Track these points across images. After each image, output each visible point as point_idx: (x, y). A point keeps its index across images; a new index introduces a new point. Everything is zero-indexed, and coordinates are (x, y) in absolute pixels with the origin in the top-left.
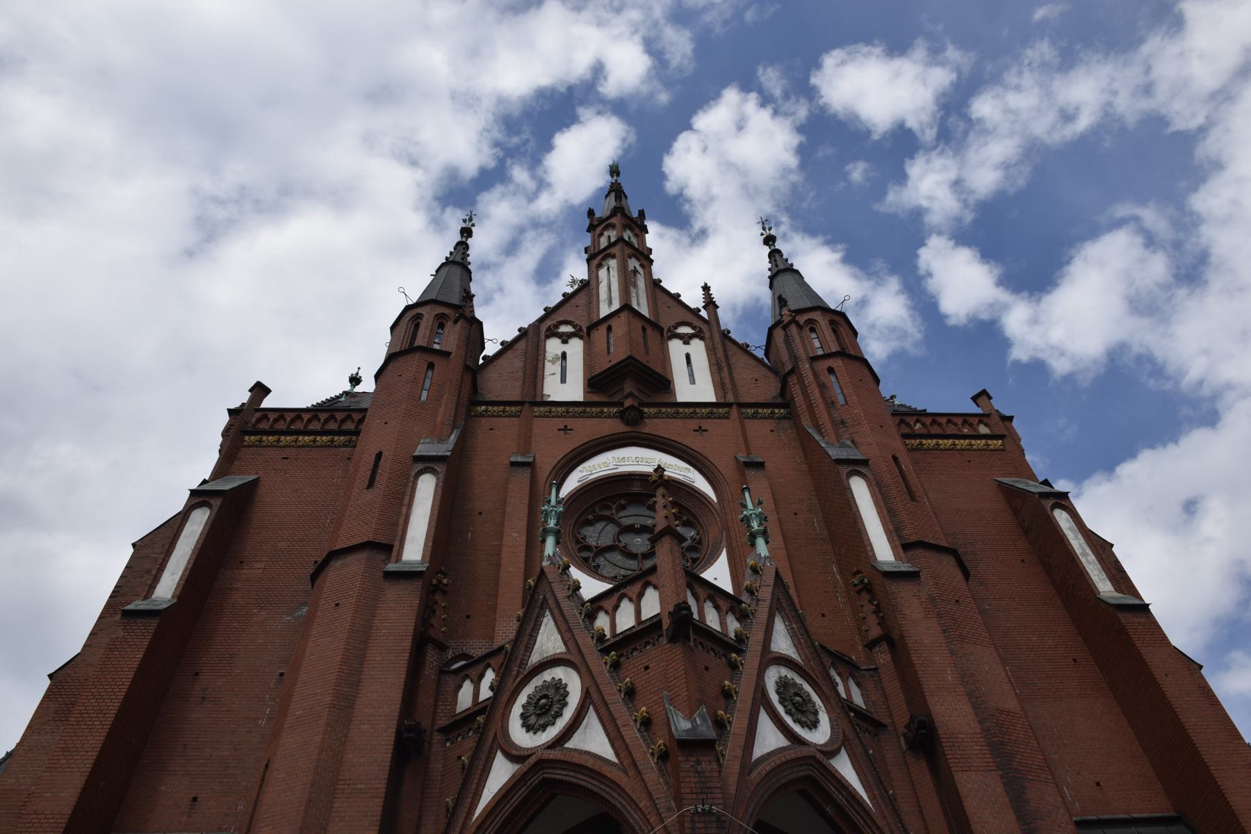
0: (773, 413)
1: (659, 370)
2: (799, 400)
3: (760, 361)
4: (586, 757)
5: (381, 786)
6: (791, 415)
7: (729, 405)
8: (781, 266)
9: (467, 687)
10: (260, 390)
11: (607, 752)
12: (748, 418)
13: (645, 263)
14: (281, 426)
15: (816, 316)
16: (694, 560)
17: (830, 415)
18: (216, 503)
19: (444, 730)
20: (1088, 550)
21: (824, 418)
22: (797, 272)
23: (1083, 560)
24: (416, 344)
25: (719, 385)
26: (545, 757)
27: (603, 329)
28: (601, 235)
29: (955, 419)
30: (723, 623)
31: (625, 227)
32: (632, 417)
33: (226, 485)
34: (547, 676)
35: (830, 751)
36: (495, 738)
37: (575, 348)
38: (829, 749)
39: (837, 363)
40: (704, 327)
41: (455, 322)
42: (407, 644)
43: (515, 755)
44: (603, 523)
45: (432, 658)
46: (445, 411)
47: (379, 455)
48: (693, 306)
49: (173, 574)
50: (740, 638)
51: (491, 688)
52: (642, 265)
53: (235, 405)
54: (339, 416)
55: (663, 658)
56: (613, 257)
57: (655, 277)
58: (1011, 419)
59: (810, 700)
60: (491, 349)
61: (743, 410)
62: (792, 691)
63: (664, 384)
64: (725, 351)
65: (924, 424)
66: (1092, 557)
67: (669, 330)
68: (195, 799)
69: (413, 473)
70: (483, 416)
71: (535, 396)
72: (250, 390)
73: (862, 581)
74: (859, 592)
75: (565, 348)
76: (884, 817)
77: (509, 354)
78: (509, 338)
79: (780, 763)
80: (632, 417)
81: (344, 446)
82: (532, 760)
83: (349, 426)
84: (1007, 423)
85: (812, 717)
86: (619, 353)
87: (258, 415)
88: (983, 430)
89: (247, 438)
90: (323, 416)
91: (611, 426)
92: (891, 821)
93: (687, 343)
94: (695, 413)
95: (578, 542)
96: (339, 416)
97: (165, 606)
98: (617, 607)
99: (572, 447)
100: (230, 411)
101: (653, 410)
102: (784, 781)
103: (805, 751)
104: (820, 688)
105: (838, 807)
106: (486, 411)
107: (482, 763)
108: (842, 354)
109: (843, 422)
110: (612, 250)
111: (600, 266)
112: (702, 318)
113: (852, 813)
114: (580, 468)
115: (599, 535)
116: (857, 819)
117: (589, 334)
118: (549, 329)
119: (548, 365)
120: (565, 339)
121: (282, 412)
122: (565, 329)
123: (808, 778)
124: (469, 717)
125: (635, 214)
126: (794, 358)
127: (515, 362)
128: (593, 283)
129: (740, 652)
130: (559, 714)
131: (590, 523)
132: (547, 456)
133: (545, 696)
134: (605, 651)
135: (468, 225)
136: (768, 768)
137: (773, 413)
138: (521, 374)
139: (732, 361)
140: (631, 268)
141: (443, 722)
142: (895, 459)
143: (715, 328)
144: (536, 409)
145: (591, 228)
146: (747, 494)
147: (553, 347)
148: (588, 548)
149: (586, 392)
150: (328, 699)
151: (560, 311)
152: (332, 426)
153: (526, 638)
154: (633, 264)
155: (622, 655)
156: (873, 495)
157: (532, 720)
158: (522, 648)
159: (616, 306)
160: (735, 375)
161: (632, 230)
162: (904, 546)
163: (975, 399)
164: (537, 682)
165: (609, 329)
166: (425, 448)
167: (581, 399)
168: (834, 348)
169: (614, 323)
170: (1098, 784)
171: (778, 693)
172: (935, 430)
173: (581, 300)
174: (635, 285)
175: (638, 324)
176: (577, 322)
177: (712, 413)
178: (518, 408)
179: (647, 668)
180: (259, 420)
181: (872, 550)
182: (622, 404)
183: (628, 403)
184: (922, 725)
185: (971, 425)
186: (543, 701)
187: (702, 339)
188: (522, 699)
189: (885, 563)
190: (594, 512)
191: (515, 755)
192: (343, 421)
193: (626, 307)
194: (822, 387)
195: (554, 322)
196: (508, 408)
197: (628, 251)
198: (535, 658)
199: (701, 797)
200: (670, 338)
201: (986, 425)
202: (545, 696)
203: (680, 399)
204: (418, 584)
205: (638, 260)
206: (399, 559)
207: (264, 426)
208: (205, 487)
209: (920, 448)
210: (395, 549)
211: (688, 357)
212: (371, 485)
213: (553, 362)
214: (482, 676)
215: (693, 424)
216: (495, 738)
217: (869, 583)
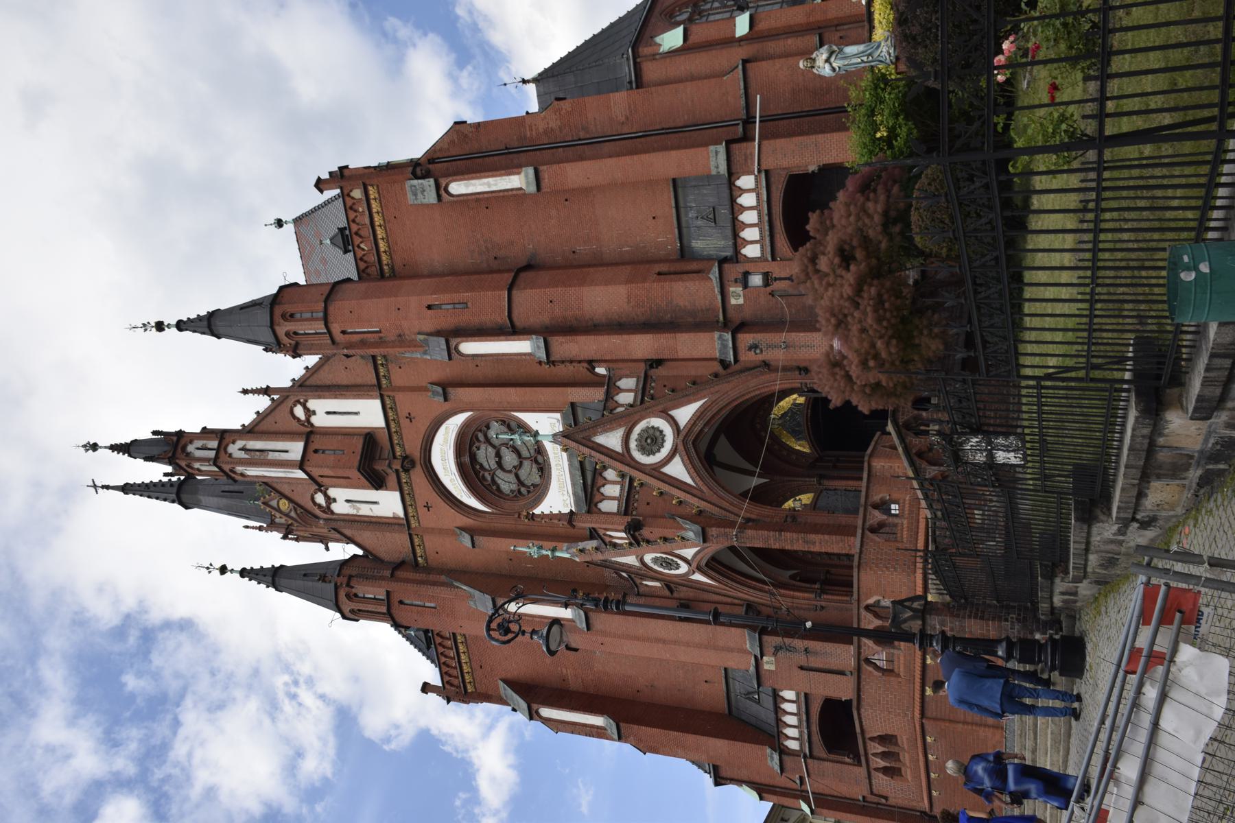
1: (358, 444)
10: (426, 688)
18: (535, 706)
23: (494, 188)
32: (408, 463)
33: (524, 705)
63: (369, 437)
66: (491, 180)
70: (426, 559)
79: (690, 465)
80: (408, 463)
91: (418, 475)
103: (681, 447)
115: (506, 483)
116: (709, 415)
118: (324, 512)
119: (361, 513)
131: (498, 487)
140: (242, 455)
141: (667, 593)
142: (429, 307)
180: (452, 685)
182: (397, 471)
193: (301, 465)
200: (312, 425)
211: (328, 413)
213: (358, 509)
215: (404, 423)
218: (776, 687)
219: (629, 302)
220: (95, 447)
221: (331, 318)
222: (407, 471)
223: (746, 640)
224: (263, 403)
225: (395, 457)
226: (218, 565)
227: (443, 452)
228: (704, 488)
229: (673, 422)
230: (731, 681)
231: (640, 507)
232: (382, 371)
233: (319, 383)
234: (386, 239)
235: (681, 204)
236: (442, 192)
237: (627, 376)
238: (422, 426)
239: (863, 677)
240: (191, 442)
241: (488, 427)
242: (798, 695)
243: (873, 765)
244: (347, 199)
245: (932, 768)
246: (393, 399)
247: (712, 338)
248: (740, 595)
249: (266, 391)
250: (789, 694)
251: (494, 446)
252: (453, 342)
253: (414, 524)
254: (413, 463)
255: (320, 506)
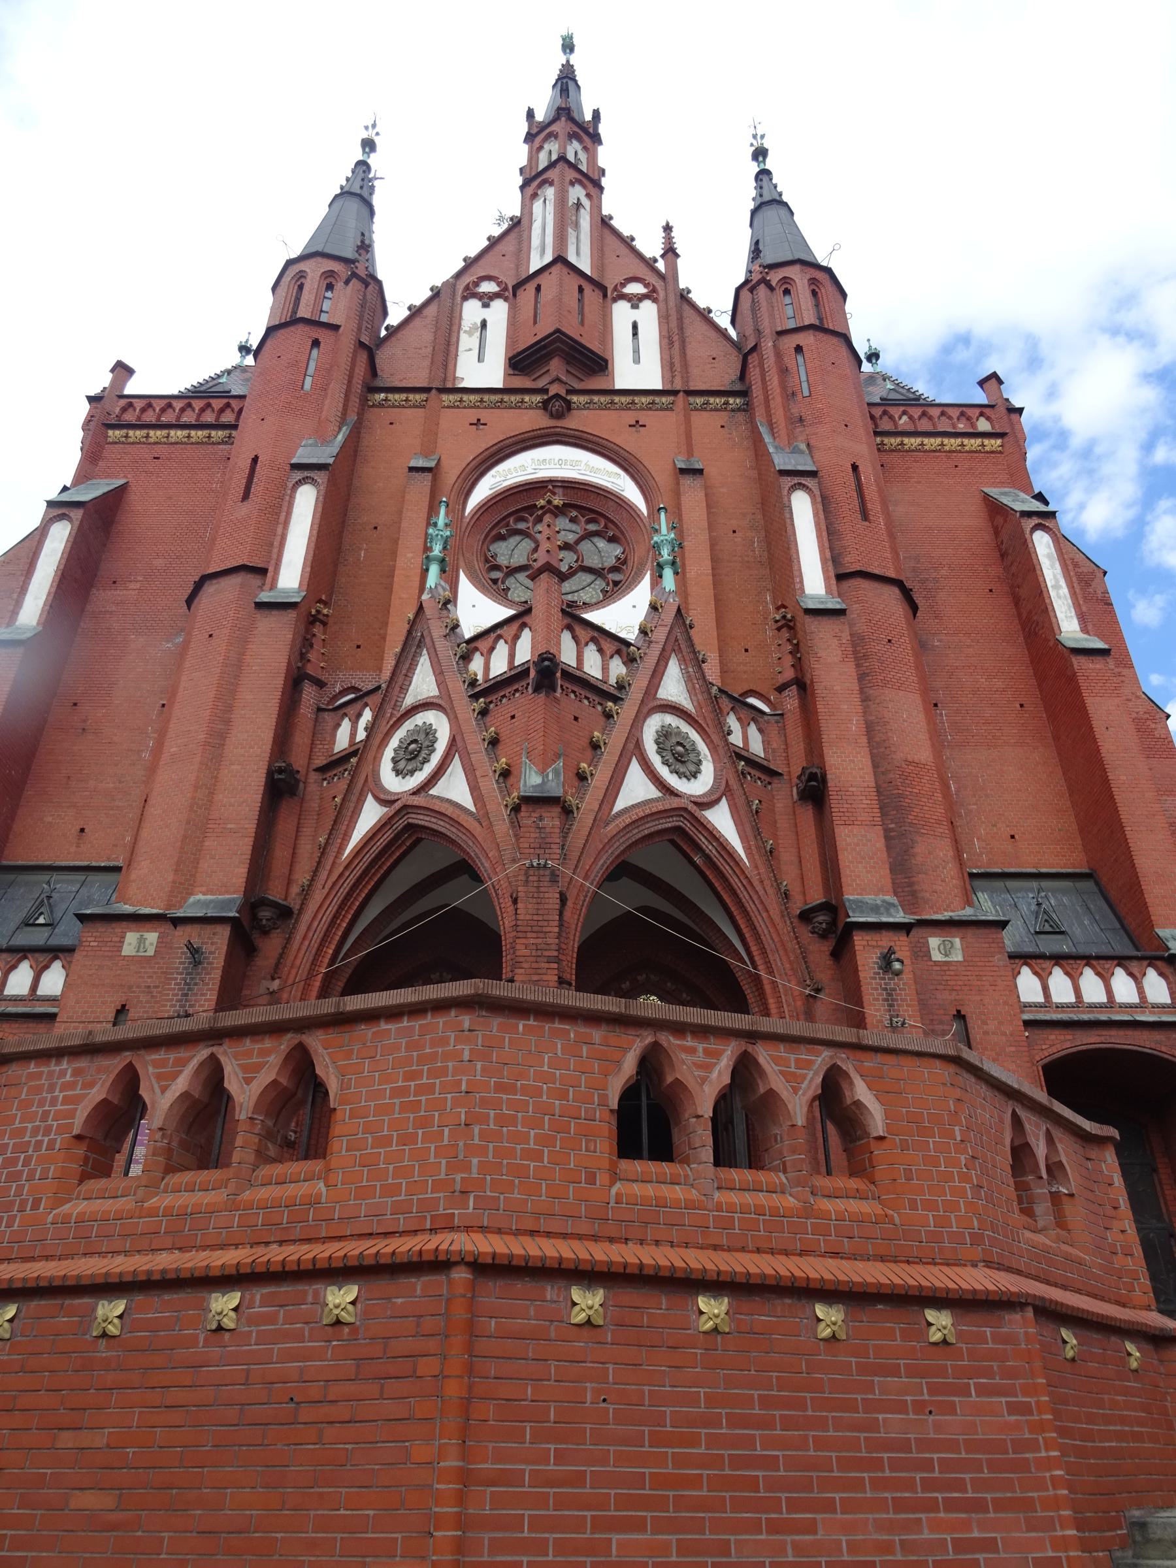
0: (727, 403)
1: (594, 346)
2: (757, 391)
3: (723, 333)
4: (446, 805)
5: (251, 826)
6: (747, 408)
7: (675, 393)
8: (767, 198)
9: (346, 725)
10: (122, 370)
11: (467, 802)
12: (696, 410)
13: (593, 191)
14: (150, 417)
15: (793, 272)
16: (616, 583)
17: (786, 409)
18: (77, 514)
19: (322, 770)
20: (1062, 583)
21: (779, 415)
22: (786, 204)
23: (1053, 594)
24: (298, 316)
25: (668, 367)
26: (410, 803)
27: (531, 287)
28: (541, 148)
29: (950, 411)
30: (605, 669)
31: (572, 136)
33: (86, 494)
34: (420, 719)
35: (707, 803)
36: (366, 780)
37: (499, 312)
38: (705, 800)
39: (807, 340)
40: (659, 284)
41: (347, 282)
42: (279, 682)
43: (385, 800)
44: (518, 538)
45: (309, 693)
46: (332, 404)
47: (255, 460)
48: (648, 254)
49: (36, 598)
50: (621, 686)
51: (366, 729)
52: (588, 195)
53: (95, 391)
54: (217, 404)
55: (525, 705)
56: (551, 184)
57: (605, 212)
58: (1020, 411)
59: (695, 750)
60: (396, 316)
61: (691, 399)
62: (674, 740)
63: (599, 364)
64: (680, 319)
65: (911, 417)
66: (1065, 590)
67: (615, 289)
68: (82, 830)
69: (290, 485)
70: (380, 406)
71: (445, 380)
72: (112, 371)
73: (784, 617)
74: (779, 629)
75: (486, 313)
76: (756, 867)
77: (417, 322)
78: (418, 302)
79: (644, 814)
81: (223, 443)
82: (397, 805)
83: (228, 418)
84: (1014, 416)
85: (692, 768)
86: (545, 328)
87: (123, 402)
88: (983, 425)
89: (110, 432)
90: (198, 404)
91: (533, 419)
92: (762, 870)
93: (635, 307)
94: (633, 403)
95: (487, 561)
96: (217, 404)
97: (29, 635)
98: (492, 649)
99: (484, 446)
100: (91, 399)
101: (583, 399)
102: (646, 832)
103: (675, 803)
104: (709, 736)
105: (708, 858)
106: (386, 400)
107: (352, 805)
108: (817, 328)
109: (801, 420)
110: (550, 174)
111: (535, 196)
112: (656, 271)
113: (720, 863)
114: (493, 472)
116: (727, 870)
117: (515, 295)
118: (467, 288)
120: (486, 300)
121: (149, 400)
122: (488, 287)
123: (678, 829)
124: (344, 758)
125: (588, 117)
126: (758, 332)
127: (422, 334)
128: (524, 222)
129: (616, 699)
130: (426, 760)
131: (501, 538)
132: (455, 456)
133: (415, 741)
134: (475, 697)
135: (371, 133)
136: (628, 821)
137: (727, 403)
138: (430, 349)
139: (688, 332)
140: (572, 200)
141: (320, 761)
142: (855, 467)
143: (671, 288)
144: (444, 397)
145: (529, 138)
146: (663, 515)
147: (472, 311)
148: (497, 567)
149: (507, 375)
150: (202, 736)
151: (482, 262)
152: (209, 418)
153: (401, 678)
154: (577, 193)
155: (491, 702)
156: (816, 515)
157: (402, 764)
158: (397, 689)
159: (548, 258)
160: (689, 352)
161: (580, 140)
162: (841, 575)
163: (982, 383)
164: (409, 725)
165: (538, 288)
166: (303, 455)
167: (499, 384)
168: (809, 318)
169: (543, 280)
170: (1013, 837)
171: (657, 742)
172: (925, 425)
173: (508, 246)
174: (577, 226)
175: (574, 282)
176: (502, 278)
177: (653, 403)
178: (424, 396)
179: (513, 717)
180: (124, 410)
181: (802, 582)
183: (554, 389)
184: (812, 777)
185: (969, 419)
186: (413, 746)
187: (655, 301)
188: (394, 742)
189: (812, 597)
190: (508, 525)
191: (385, 800)
192: (222, 410)
193: (560, 260)
194: (784, 371)
195: (474, 278)
196: (411, 397)
197: (571, 174)
198: (409, 701)
199: (538, 851)
200: (615, 300)
201: (988, 419)
202: (415, 741)
203: (619, 385)
204: (291, 615)
205: (584, 187)
206: (273, 586)
207: (130, 417)
208: (66, 497)
209: (899, 450)
210: (270, 574)
211: (635, 326)
212: (246, 496)
214: (359, 715)
215: (630, 417)
216: (366, 780)
217: (792, 621)
218: (78, 956)
219: (910, 763)
220: (568, 46)
221: (820, 335)
222: (545, 405)
223: (219, 888)
224: (651, 247)
225: (569, 392)
226: (377, 140)
227: (574, 464)
228: (612, 829)
229: (707, 803)
230: (80, 877)
231: (569, 703)
232: (718, 401)
233: (686, 321)
234: (921, 449)
235: (1045, 884)
236: (1035, 521)
237: (766, 743)
238: (626, 440)
239: (597, 1034)
240: (585, 148)
241: (612, 540)
242: (51, 1000)
243: (149, 1066)
244: (977, 411)
245: (157, 1308)
246: (668, 408)
247: (881, 890)
248: (318, 896)
249: (670, 252)
250: (54, 981)
251: (578, 542)
252: (809, 482)
253: (447, 398)
254: (559, 416)
255: (477, 284)
